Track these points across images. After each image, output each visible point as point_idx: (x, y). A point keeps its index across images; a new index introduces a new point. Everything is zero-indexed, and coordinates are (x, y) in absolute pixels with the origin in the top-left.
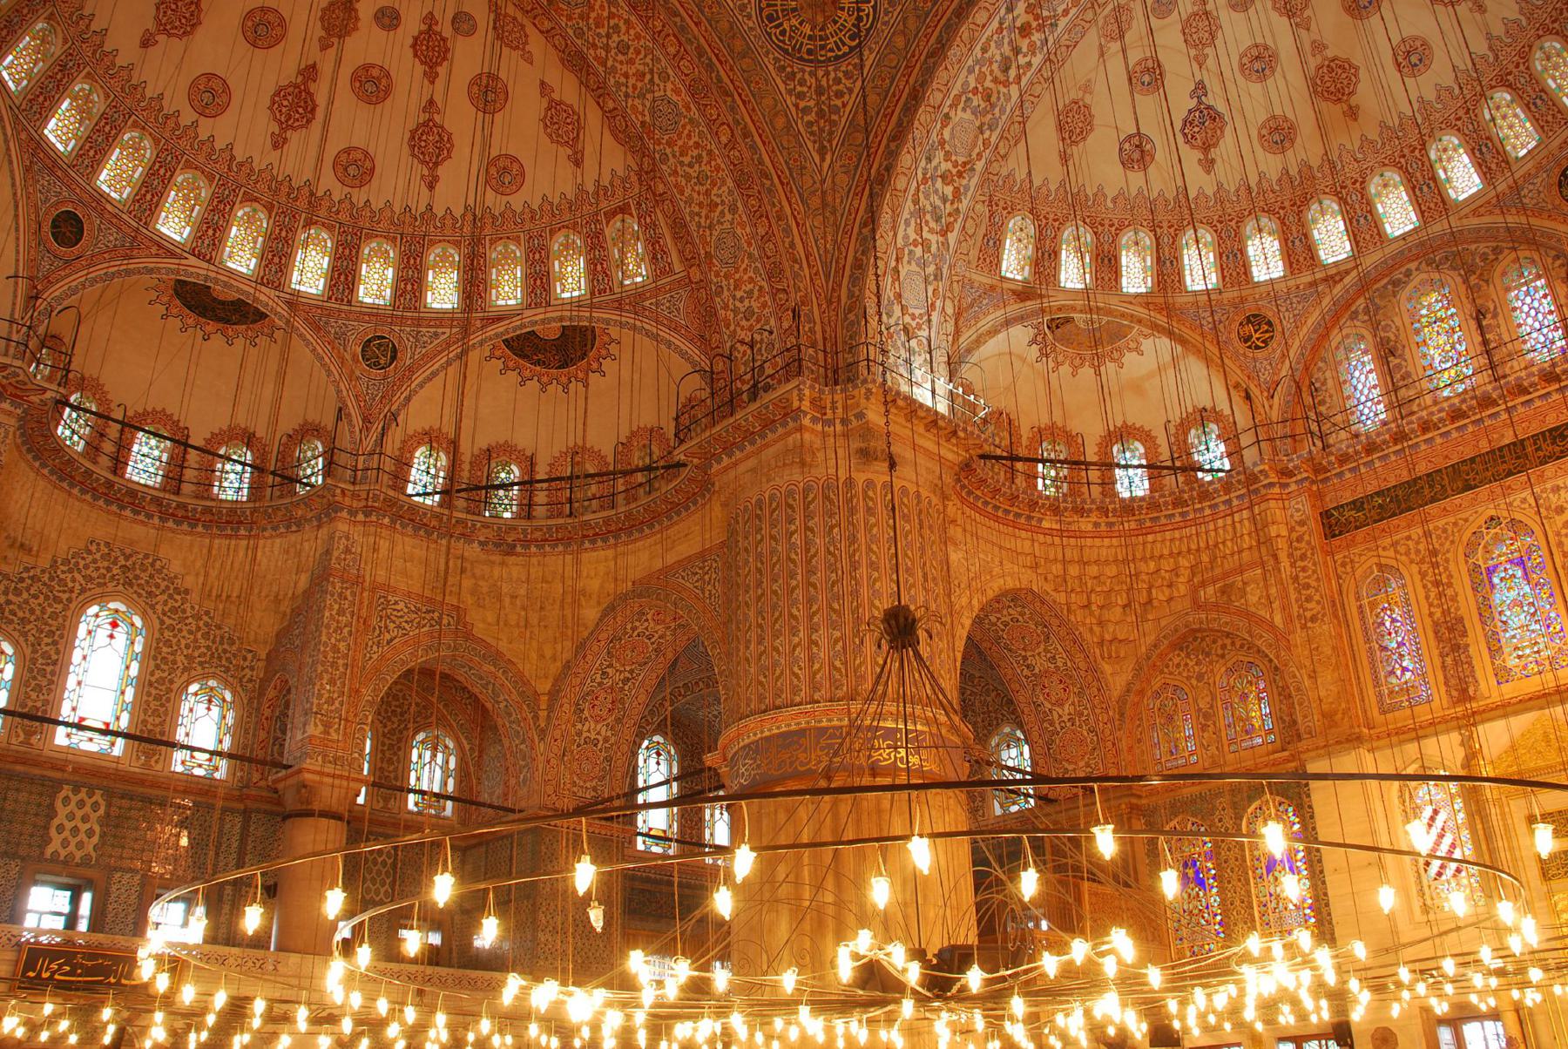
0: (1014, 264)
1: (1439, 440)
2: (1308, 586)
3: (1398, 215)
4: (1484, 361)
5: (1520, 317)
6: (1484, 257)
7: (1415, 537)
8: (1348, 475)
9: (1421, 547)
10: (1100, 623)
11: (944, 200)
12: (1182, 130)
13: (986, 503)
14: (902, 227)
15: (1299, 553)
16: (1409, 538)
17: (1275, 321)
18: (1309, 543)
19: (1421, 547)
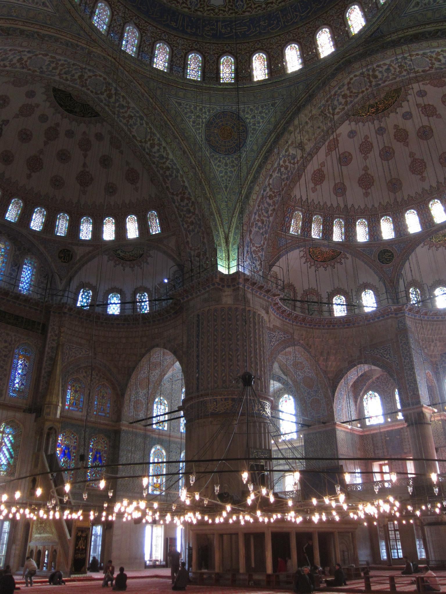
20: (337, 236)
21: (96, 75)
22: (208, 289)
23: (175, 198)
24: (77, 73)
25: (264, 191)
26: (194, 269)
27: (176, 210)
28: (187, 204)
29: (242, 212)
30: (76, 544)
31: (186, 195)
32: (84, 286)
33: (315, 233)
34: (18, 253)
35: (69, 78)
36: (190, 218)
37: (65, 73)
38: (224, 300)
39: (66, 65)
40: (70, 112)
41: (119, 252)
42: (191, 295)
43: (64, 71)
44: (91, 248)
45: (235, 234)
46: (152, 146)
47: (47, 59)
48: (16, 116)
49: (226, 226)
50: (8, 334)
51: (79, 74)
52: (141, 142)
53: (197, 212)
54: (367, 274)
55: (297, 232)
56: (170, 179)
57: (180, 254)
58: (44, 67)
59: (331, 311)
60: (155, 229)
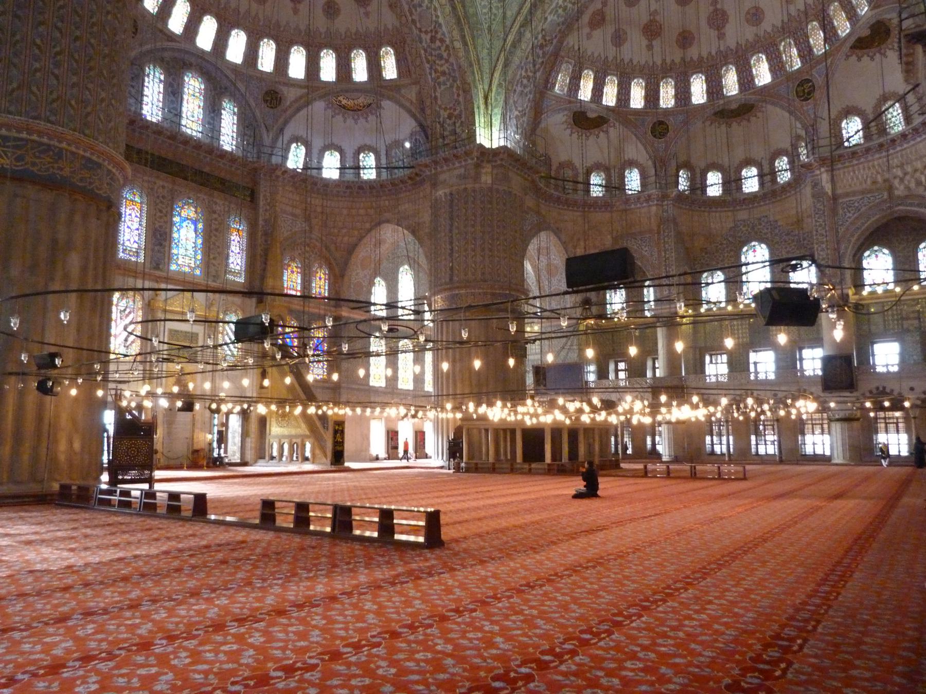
20: (610, 97)
22: (463, 163)
23: (423, 36)
25: (536, 38)
26: (444, 136)
27: (422, 52)
28: (439, 48)
29: (506, 65)
30: (335, 438)
31: (439, 36)
32: (296, 139)
33: (585, 92)
34: (213, 93)
36: (442, 66)
38: (483, 178)
41: (341, 98)
42: (442, 167)
45: (498, 93)
49: (487, 81)
50: (216, 203)
53: (452, 60)
54: (635, 150)
55: (563, 91)
57: (423, 110)
59: (588, 191)
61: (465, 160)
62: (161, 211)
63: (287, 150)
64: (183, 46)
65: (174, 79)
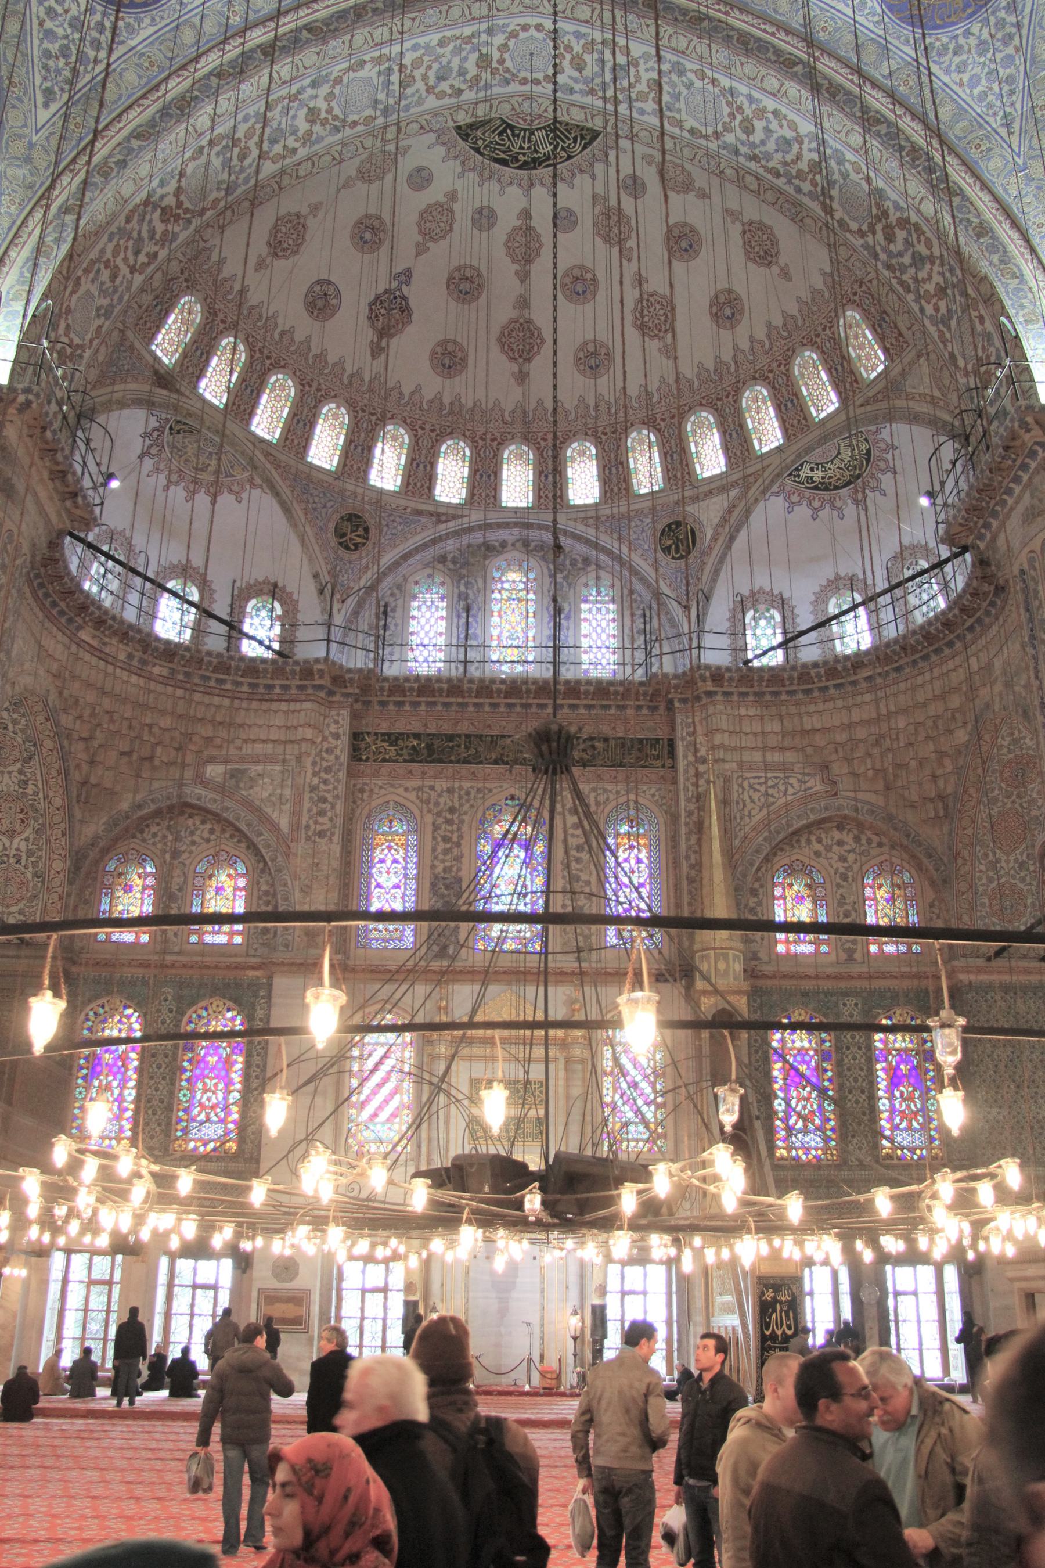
0: (167, 345)
1: (487, 708)
2: (324, 800)
3: (517, 486)
4: (549, 654)
5: (585, 629)
6: (573, 562)
7: (438, 787)
8: (391, 707)
9: (442, 800)
10: (92, 763)
11: (152, 233)
12: (372, 304)
13: (41, 585)
14: (105, 238)
15: (325, 764)
16: (432, 788)
17: (373, 531)
18: (337, 758)
19: (442, 800)
21: (513, 35)
24: (466, 59)
31: (893, 218)
35: (457, 83)
36: (930, 278)
37: (441, 78)
39: (426, 58)
40: (534, 163)
42: (994, 514)
43: (431, 74)
44: (734, 493)
46: (749, 130)
47: (369, 72)
48: (421, 250)
51: (473, 57)
52: (717, 135)
56: (835, 193)
58: (382, 97)
60: (872, 362)
61: (1024, 467)
62: (446, 839)
63: (737, 631)
64: (476, 517)
65: (467, 584)
